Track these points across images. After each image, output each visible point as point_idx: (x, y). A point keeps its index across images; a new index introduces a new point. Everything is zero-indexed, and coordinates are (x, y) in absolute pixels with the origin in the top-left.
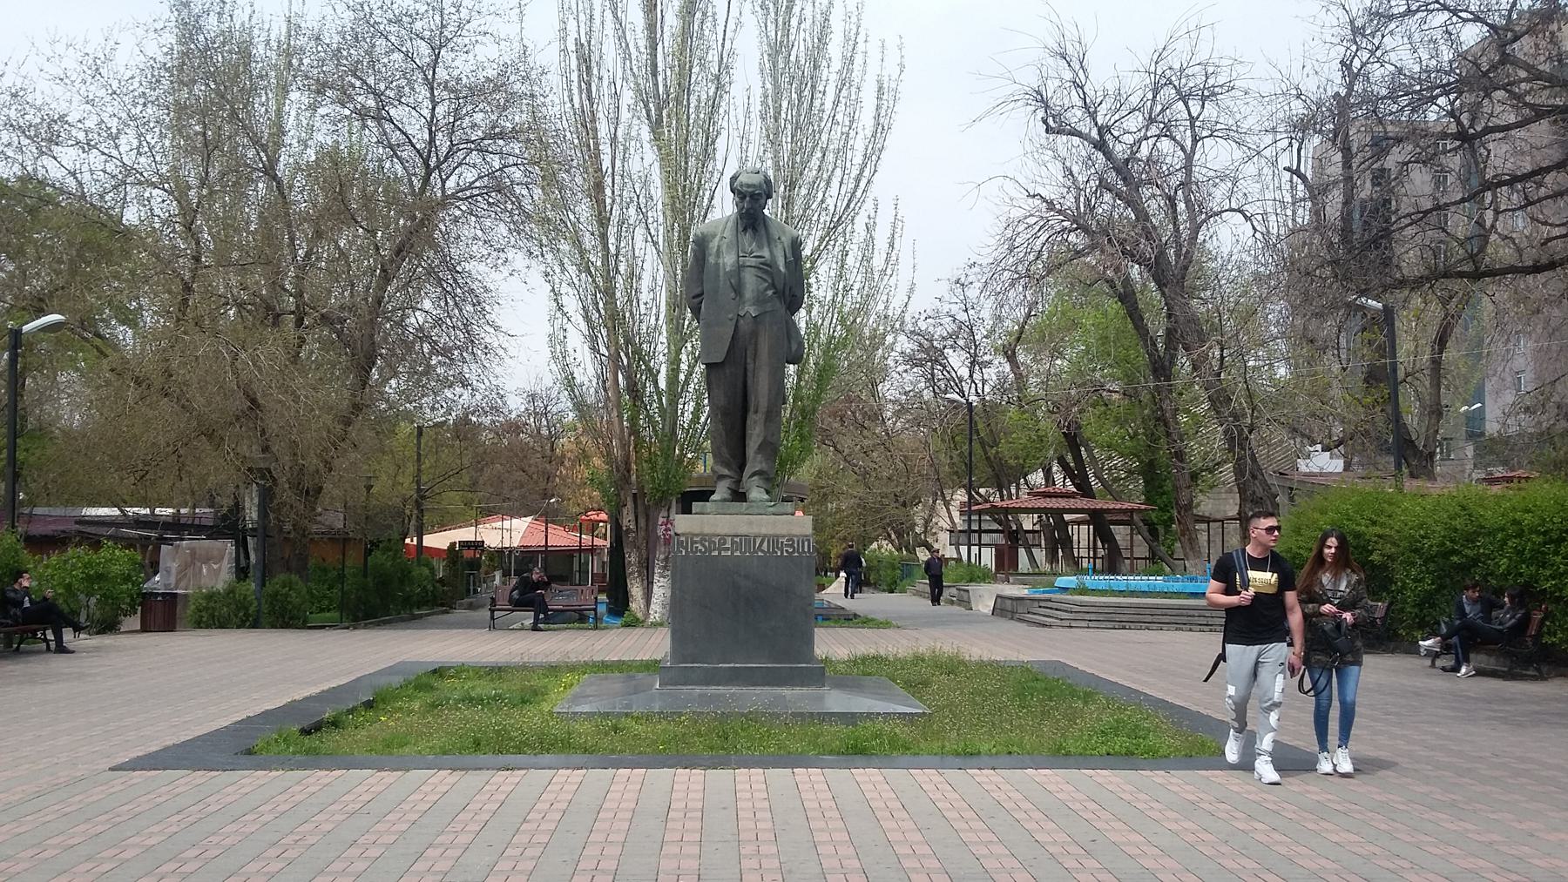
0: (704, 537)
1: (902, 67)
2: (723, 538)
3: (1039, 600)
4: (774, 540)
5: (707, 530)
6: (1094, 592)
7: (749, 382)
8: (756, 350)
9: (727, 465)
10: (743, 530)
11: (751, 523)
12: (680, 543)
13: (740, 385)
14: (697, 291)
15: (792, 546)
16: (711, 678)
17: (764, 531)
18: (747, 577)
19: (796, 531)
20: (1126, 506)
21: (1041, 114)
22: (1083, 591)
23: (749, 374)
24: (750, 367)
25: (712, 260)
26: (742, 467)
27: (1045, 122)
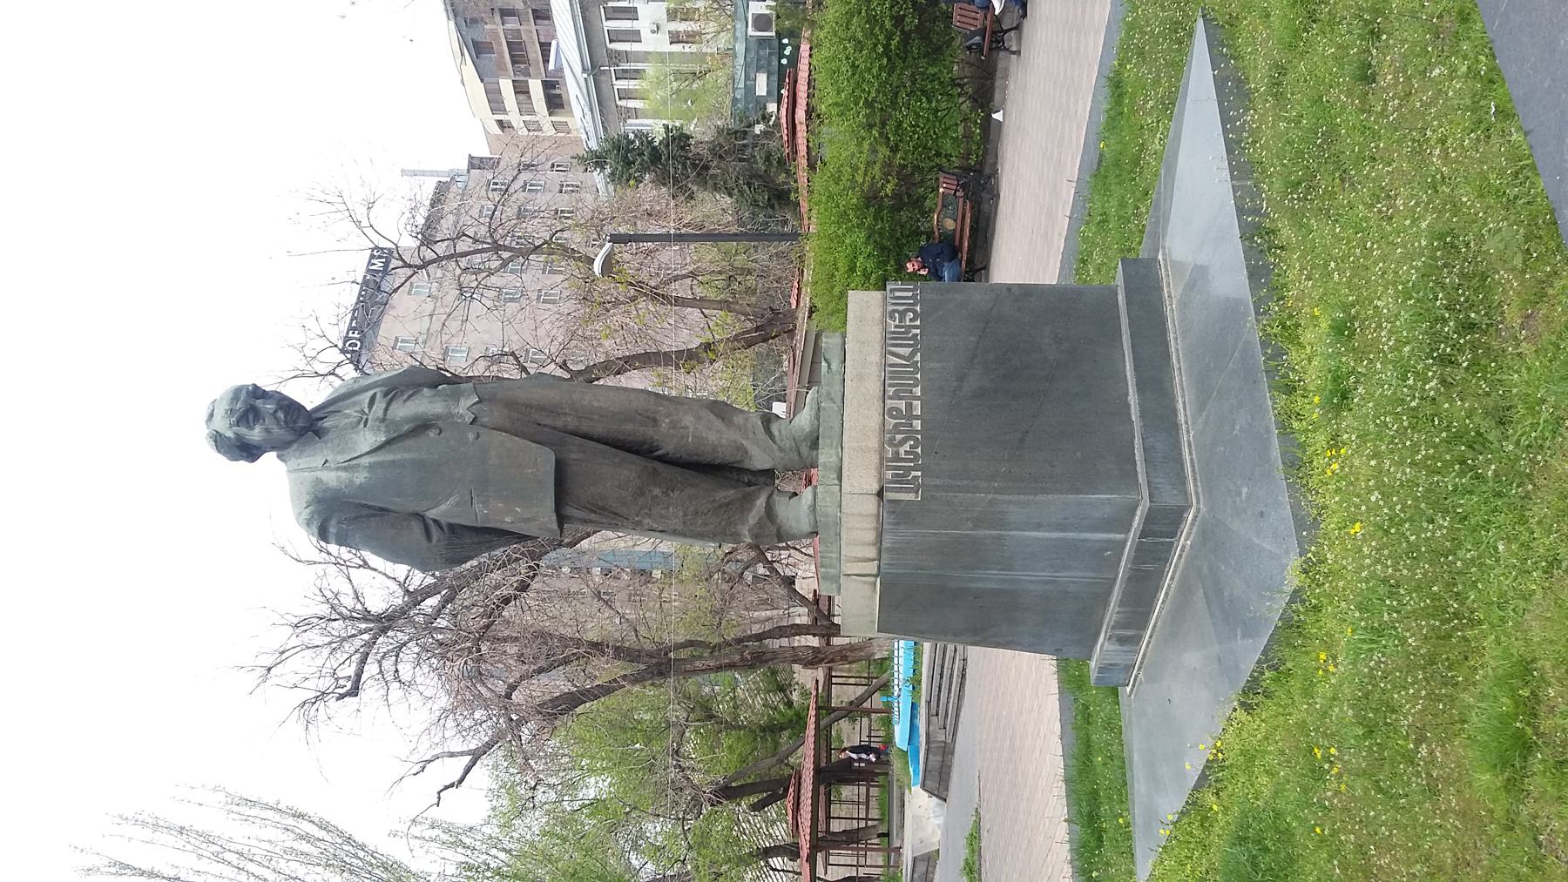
0: (887, 438)
1: (215, 790)
2: (886, 412)
3: (929, 715)
4: (890, 340)
5: (873, 442)
6: (916, 671)
7: (599, 429)
8: (541, 408)
9: (748, 501)
10: (873, 387)
11: (860, 377)
14: (417, 529)
15: (903, 314)
16: (1162, 418)
17: (875, 357)
18: (961, 378)
19: (876, 313)
20: (812, 712)
21: (332, 703)
22: (915, 683)
23: (585, 427)
24: (571, 422)
25: (360, 478)
27: (342, 697)
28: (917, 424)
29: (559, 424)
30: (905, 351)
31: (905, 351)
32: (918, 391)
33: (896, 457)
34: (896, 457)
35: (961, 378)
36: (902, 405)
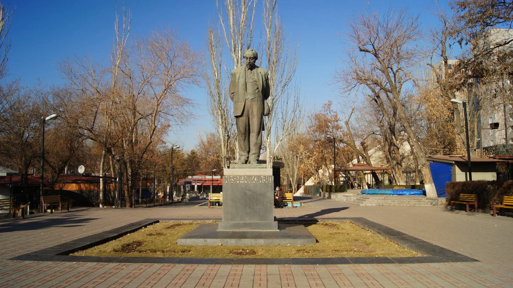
2: (241, 176)
4: (259, 177)
5: (236, 174)
7: (250, 122)
10: (248, 174)
12: (226, 178)
13: (247, 123)
17: (255, 174)
18: (249, 190)
23: (250, 119)
24: (250, 117)
26: (249, 152)
28: (238, 182)
29: (250, 114)
30: (256, 179)
31: (256, 179)
32: (246, 182)
33: (230, 178)
34: (230, 178)
35: (249, 190)
36: (242, 179)
